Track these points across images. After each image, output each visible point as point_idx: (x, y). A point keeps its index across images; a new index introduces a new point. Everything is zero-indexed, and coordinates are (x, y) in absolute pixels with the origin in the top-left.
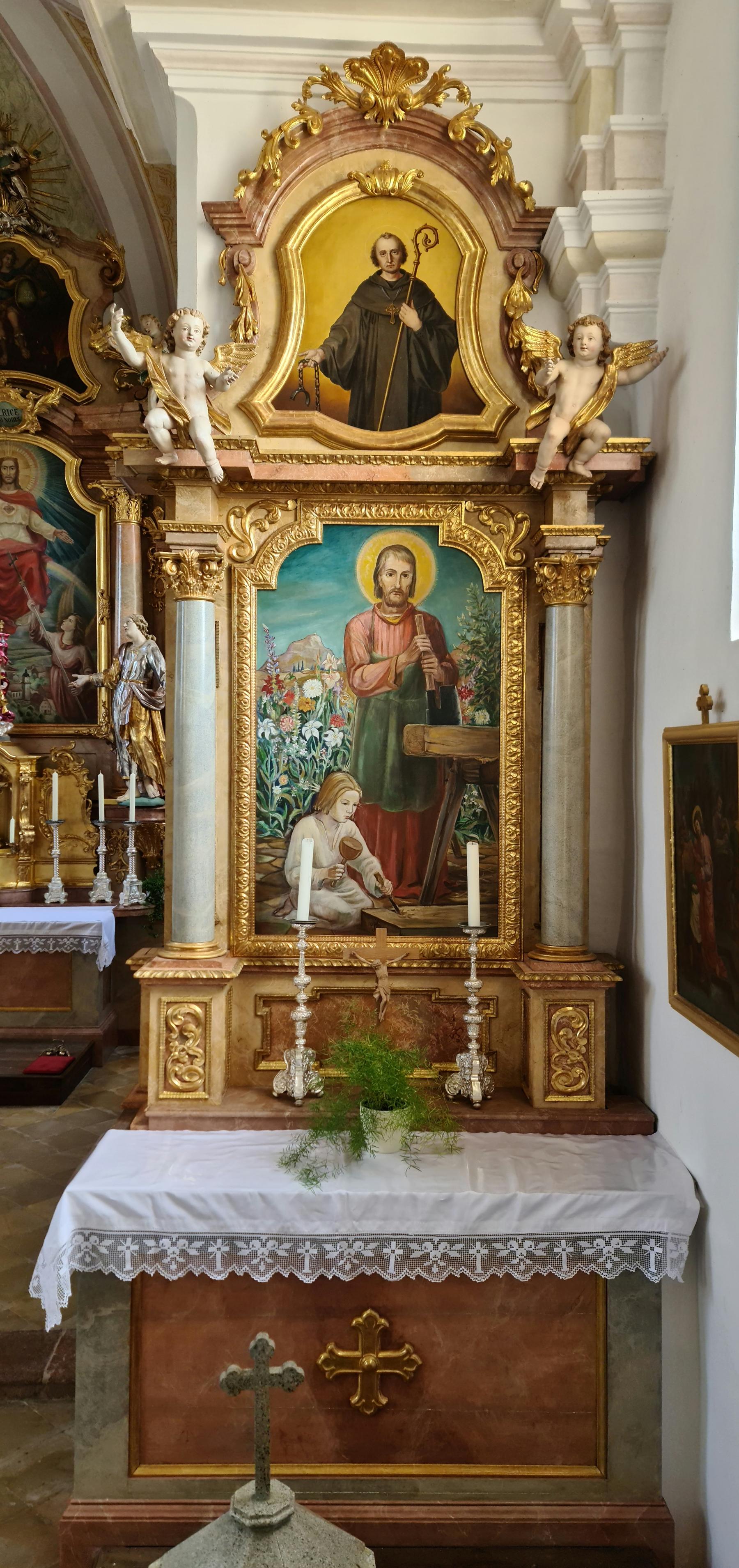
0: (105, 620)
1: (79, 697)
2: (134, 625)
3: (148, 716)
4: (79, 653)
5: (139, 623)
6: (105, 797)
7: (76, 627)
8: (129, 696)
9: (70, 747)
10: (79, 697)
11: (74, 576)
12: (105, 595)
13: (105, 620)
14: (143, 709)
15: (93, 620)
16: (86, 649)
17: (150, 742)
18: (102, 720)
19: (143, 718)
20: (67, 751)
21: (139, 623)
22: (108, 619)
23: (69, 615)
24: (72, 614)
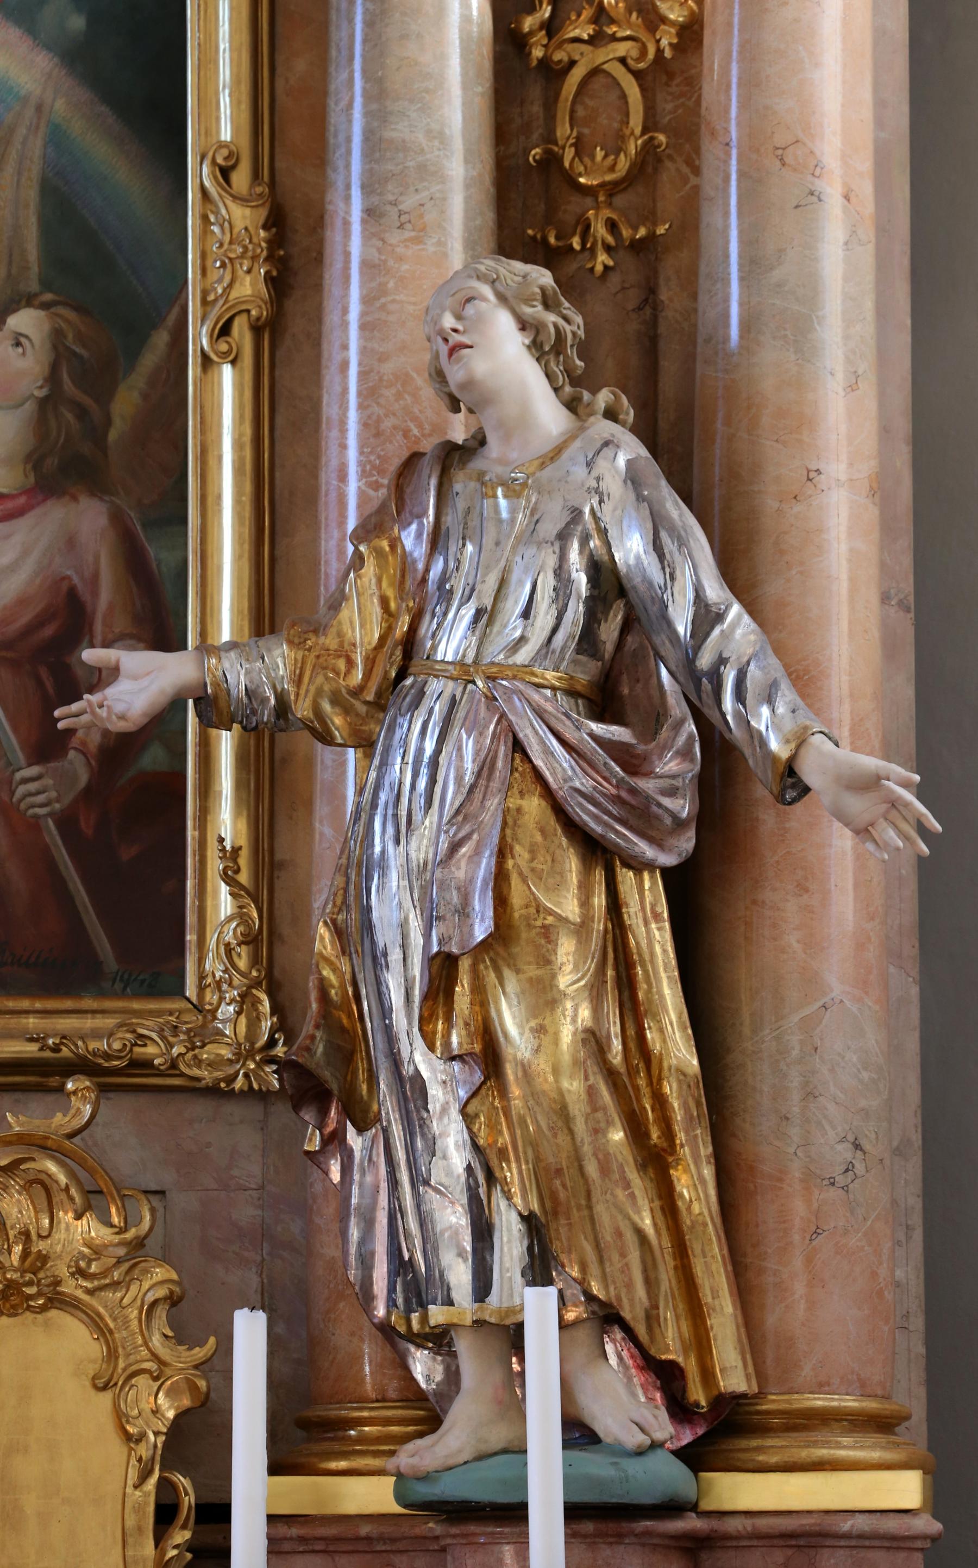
0: (241, 329)
1: (66, 822)
2: (504, 322)
3: (599, 901)
4: (71, 543)
5: (536, 311)
6: (275, 1469)
7: (53, 378)
8: (485, 768)
9: (61, 1122)
10: (66, 822)
11: (43, 61)
12: (241, 178)
13: (241, 332)
14: (572, 863)
15: (161, 339)
16: (117, 519)
17: (610, 1074)
18: (214, 966)
19: (570, 908)
20: (43, 1145)
21: (536, 311)
22: (257, 329)
23: (12, 306)
24: (29, 301)
